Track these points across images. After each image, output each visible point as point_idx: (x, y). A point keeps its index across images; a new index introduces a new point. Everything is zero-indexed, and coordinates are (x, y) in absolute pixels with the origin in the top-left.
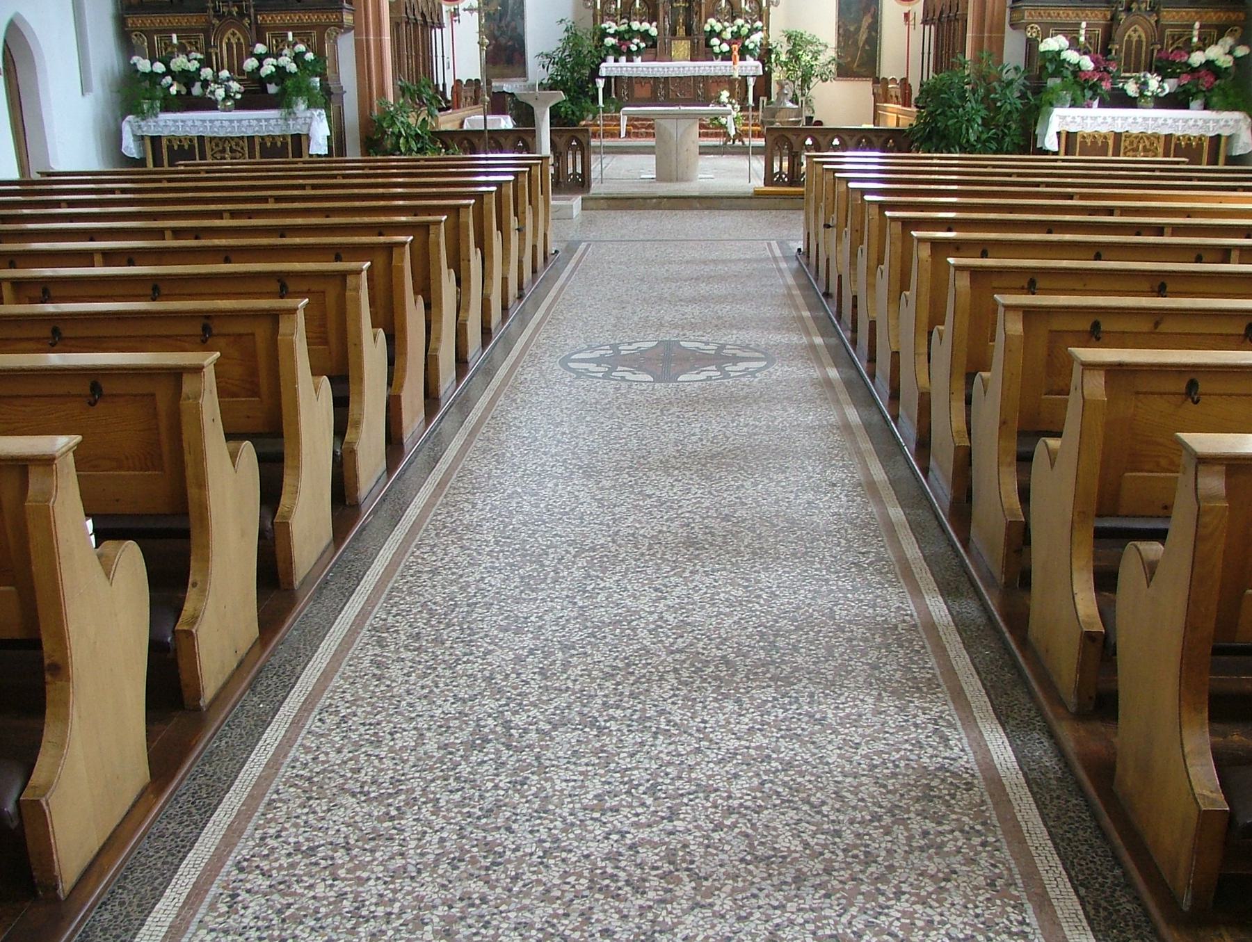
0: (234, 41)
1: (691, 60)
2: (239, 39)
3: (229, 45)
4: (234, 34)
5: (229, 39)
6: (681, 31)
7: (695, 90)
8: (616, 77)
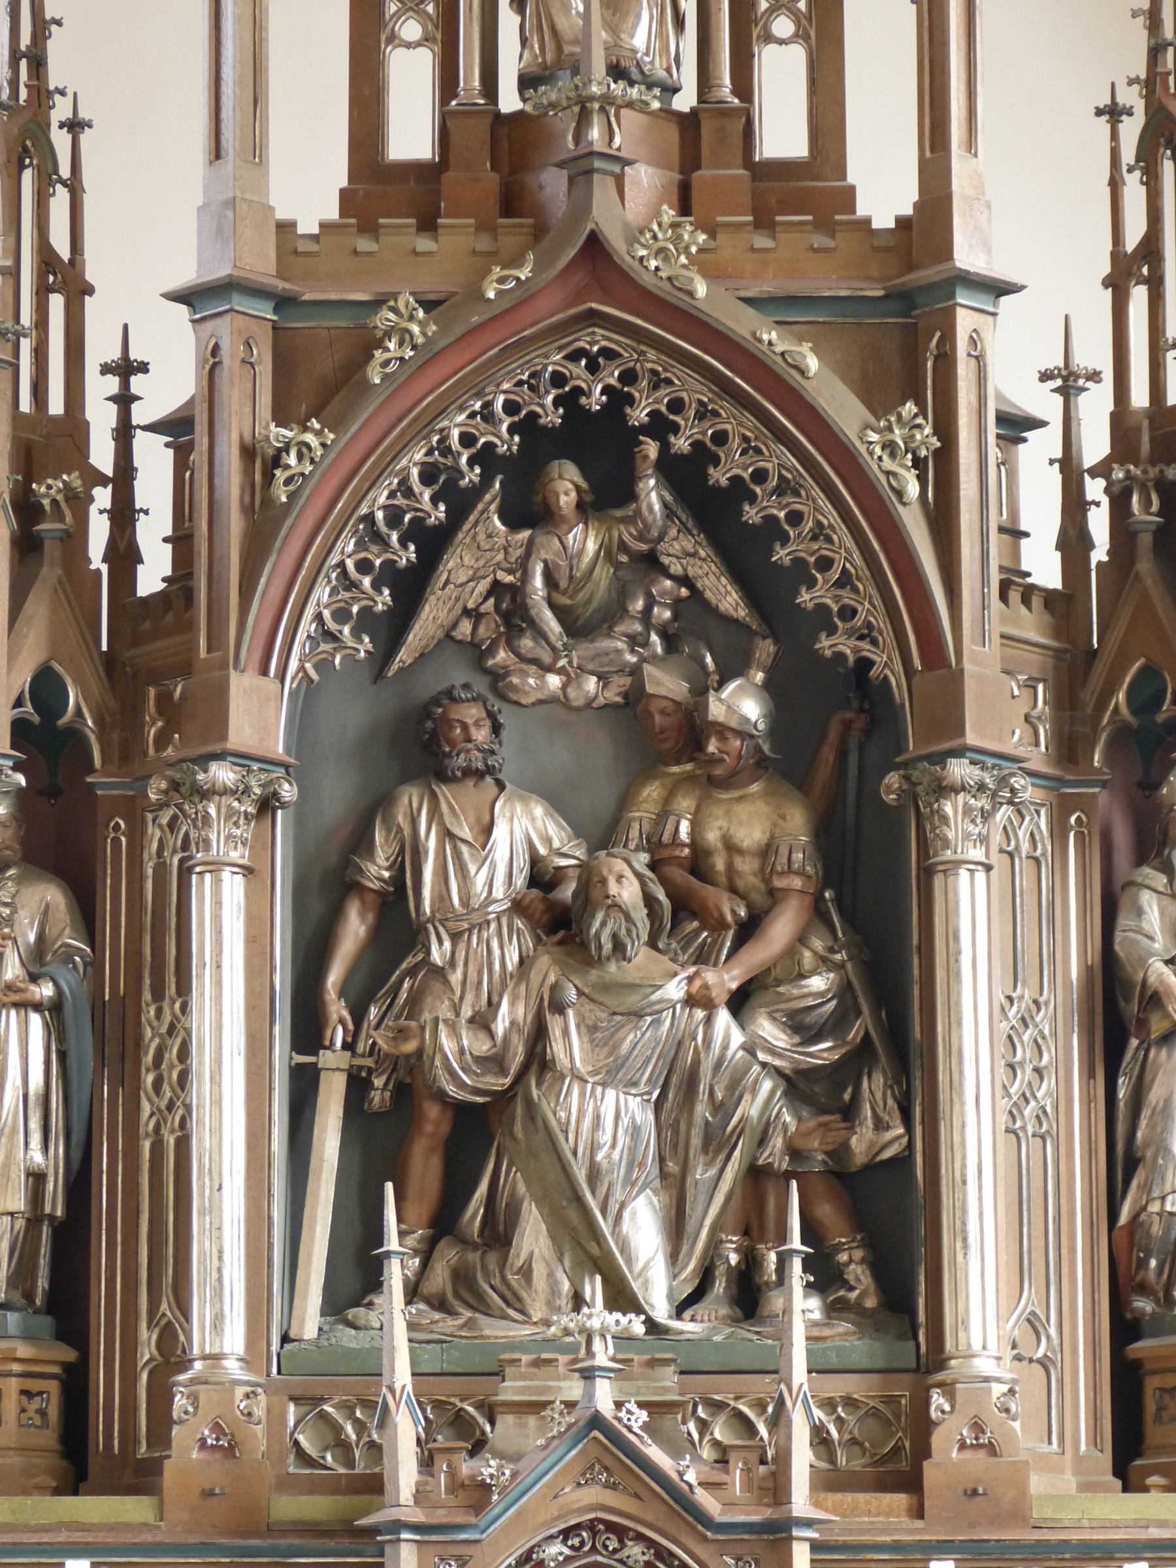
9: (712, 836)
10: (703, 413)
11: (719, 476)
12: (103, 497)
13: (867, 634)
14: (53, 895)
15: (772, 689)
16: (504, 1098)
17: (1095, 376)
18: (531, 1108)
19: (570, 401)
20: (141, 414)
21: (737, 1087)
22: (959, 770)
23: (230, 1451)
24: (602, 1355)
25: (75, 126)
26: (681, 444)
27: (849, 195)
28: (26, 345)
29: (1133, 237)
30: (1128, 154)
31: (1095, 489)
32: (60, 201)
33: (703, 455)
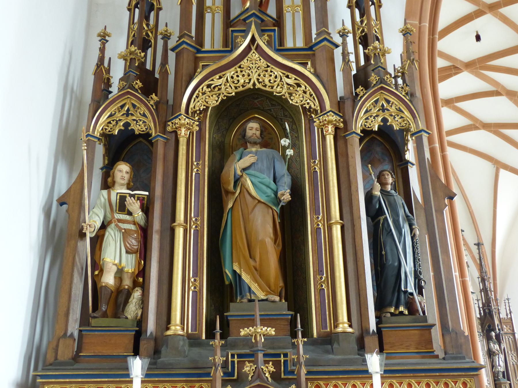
17: (480, 300)
29: (481, 289)
30: (480, 281)
31: (481, 309)
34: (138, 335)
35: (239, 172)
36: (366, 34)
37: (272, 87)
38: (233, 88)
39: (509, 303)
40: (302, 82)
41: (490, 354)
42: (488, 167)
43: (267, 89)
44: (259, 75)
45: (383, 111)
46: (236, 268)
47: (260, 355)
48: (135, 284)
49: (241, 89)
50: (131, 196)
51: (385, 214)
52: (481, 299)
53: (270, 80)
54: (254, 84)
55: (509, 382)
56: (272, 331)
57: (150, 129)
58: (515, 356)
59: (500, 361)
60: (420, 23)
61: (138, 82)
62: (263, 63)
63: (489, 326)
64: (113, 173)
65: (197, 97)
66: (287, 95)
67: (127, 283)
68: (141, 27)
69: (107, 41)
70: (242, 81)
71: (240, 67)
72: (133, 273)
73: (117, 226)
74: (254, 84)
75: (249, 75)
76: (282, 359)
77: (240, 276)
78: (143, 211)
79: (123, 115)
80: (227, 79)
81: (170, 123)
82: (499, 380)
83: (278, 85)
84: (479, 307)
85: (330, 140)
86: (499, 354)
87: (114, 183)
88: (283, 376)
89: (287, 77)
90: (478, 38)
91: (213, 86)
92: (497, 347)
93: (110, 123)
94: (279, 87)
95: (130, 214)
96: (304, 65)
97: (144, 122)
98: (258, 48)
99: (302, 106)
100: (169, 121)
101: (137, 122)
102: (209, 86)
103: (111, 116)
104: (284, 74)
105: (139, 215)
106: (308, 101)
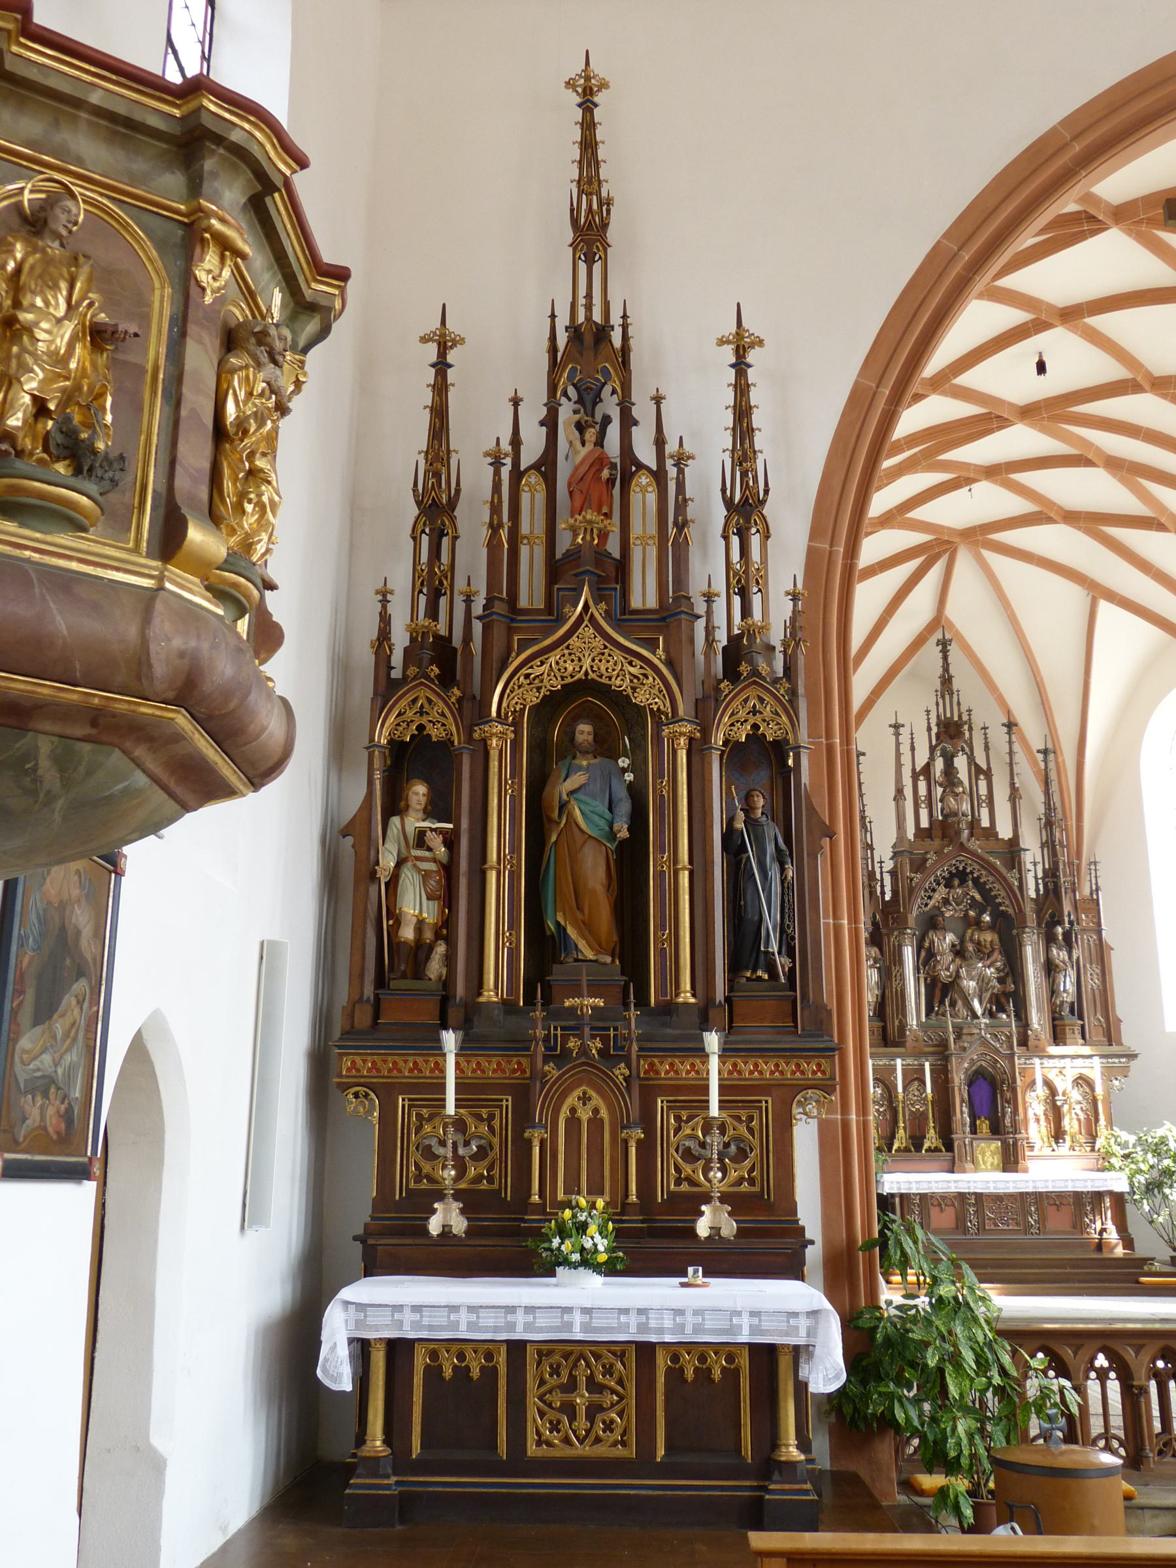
0: (585, 1115)
1: (1005, 1170)
2: (596, 1111)
3: (573, 1122)
4: (585, 1099)
5: (573, 1110)
6: (984, 1126)
7: (1025, 1219)
8: (902, 1196)
9: (982, 940)
10: (971, 865)
11: (982, 881)
12: (879, 884)
13: (1007, 906)
14: (876, 949)
15: (990, 915)
16: (952, 983)
18: (958, 985)
19: (957, 868)
20: (884, 870)
21: (989, 981)
22: (1027, 930)
23: (917, 1041)
24: (983, 1026)
25: (870, 822)
26: (975, 875)
27: (997, 834)
28: (870, 860)
29: (1044, 840)
31: (1040, 881)
32: (869, 834)
33: (979, 877)
34: (445, 1001)
35: (565, 797)
36: (743, 587)
37: (610, 678)
38: (559, 679)
39: (1096, 870)
40: (649, 672)
41: (1050, 969)
42: (1074, 594)
43: (604, 680)
44: (593, 660)
45: (754, 715)
46: (560, 919)
47: (587, 1030)
48: (438, 936)
49: (569, 680)
50: (432, 830)
51: (748, 852)
52: (1041, 861)
53: (607, 669)
54: (586, 674)
55: (1082, 1023)
56: (600, 1002)
57: (452, 735)
58: (1097, 974)
59: (1067, 984)
60: (831, 546)
61: (434, 668)
62: (599, 642)
63: (1052, 916)
64: (407, 796)
65: (512, 692)
66: (629, 691)
67: (428, 936)
68: (431, 572)
69: (389, 601)
70: (570, 669)
71: (568, 648)
72: (436, 924)
73: (415, 866)
74: (586, 674)
75: (580, 660)
76: (612, 1033)
77: (565, 930)
78: (445, 846)
79: (415, 713)
80: (551, 666)
81: (476, 728)
82: (1062, 1018)
83: (618, 676)
84: (1036, 878)
85: (682, 756)
86: (1066, 970)
87: (407, 807)
88: (612, 1052)
89: (630, 663)
90: (1041, 368)
91: (532, 676)
92: (1064, 955)
93: (398, 725)
94: (619, 679)
95: (430, 849)
96: (652, 645)
97: (443, 725)
98: (592, 619)
99: (649, 705)
100: (477, 725)
101: (434, 725)
102: (527, 676)
103: (399, 714)
104: (626, 659)
105: (441, 851)
106: (657, 700)
